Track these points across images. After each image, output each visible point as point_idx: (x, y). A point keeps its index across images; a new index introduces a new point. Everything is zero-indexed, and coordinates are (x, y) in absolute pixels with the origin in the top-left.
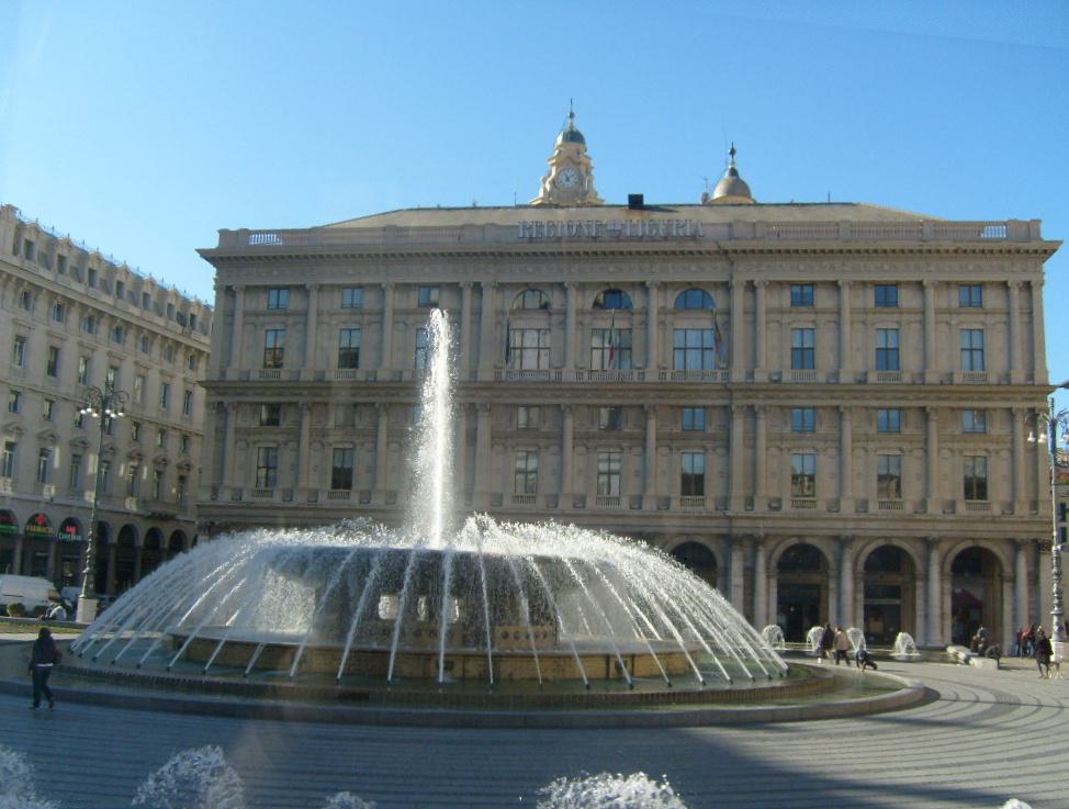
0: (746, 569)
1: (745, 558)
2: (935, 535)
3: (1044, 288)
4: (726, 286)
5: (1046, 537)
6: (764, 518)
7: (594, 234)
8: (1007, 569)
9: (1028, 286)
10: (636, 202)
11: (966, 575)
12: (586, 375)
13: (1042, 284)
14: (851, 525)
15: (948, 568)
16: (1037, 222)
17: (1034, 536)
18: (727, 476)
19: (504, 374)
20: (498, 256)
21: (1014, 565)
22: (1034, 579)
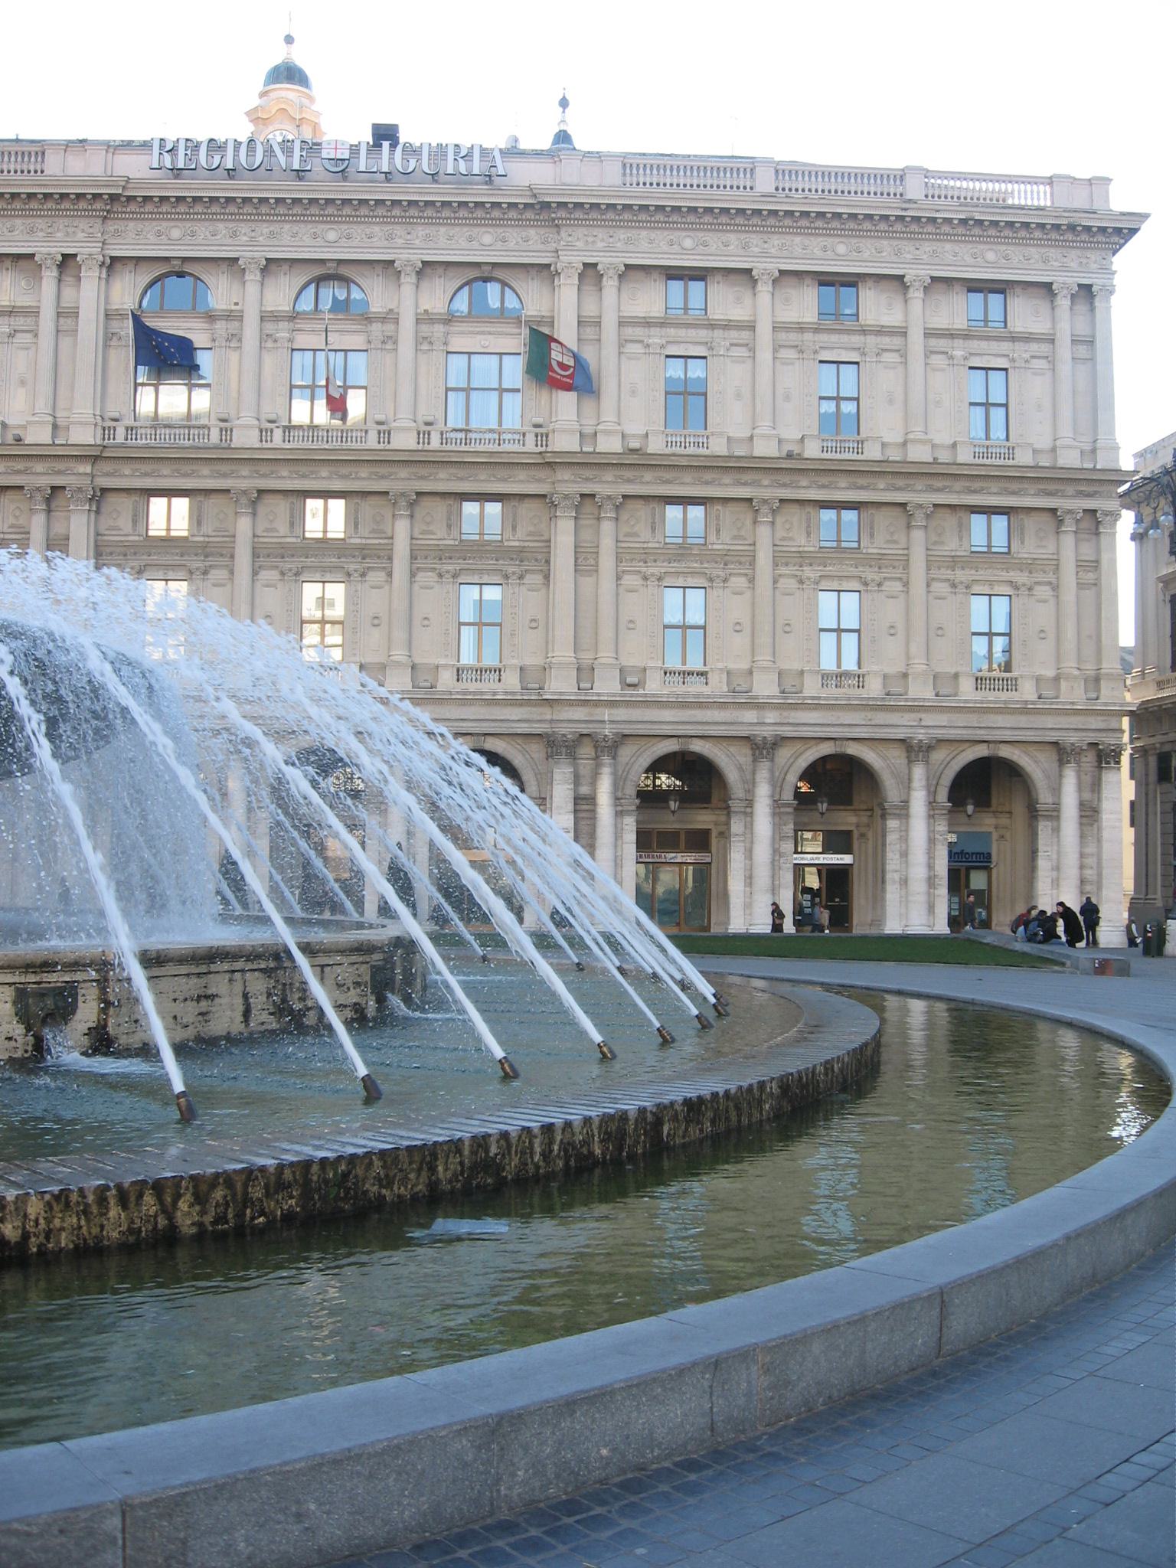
0: (578, 800)
1: (577, 780)
2: (921, 735)
3: (1114, 299)
4: (545, 271)
5: (1109, 740)
6: (612, 704)
7: (296, 166)
8: (1044, 797)
9: (1086, 292)
10: (384, 134)
11: (970, 808)
12: (278, 434)
13: (1111, 293)
14: (771, 717)
15: (943, 795)
16: (1107, 181)
17: (1092, 737)
18: (542, 624)
19: (121, 433)
20: (113, 203)
21: (1057, 790)
22: (1090, 813)
